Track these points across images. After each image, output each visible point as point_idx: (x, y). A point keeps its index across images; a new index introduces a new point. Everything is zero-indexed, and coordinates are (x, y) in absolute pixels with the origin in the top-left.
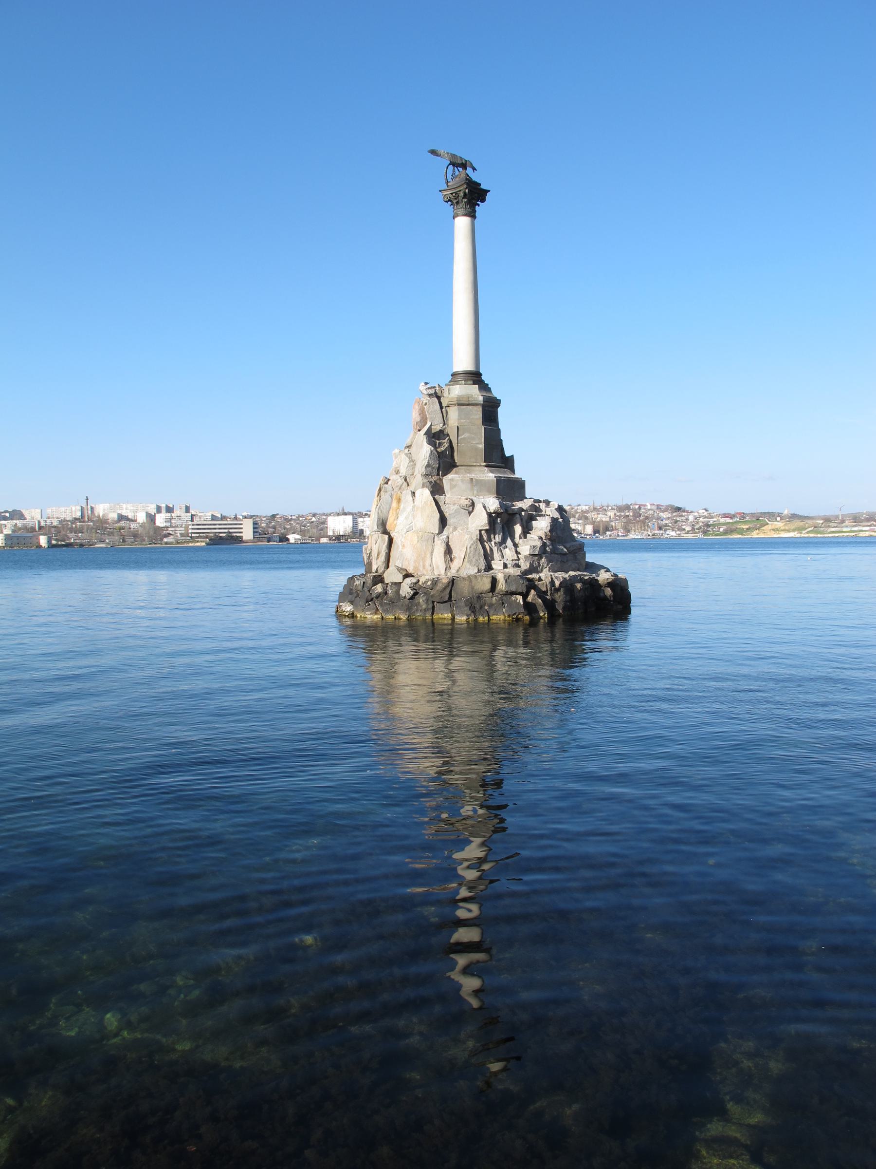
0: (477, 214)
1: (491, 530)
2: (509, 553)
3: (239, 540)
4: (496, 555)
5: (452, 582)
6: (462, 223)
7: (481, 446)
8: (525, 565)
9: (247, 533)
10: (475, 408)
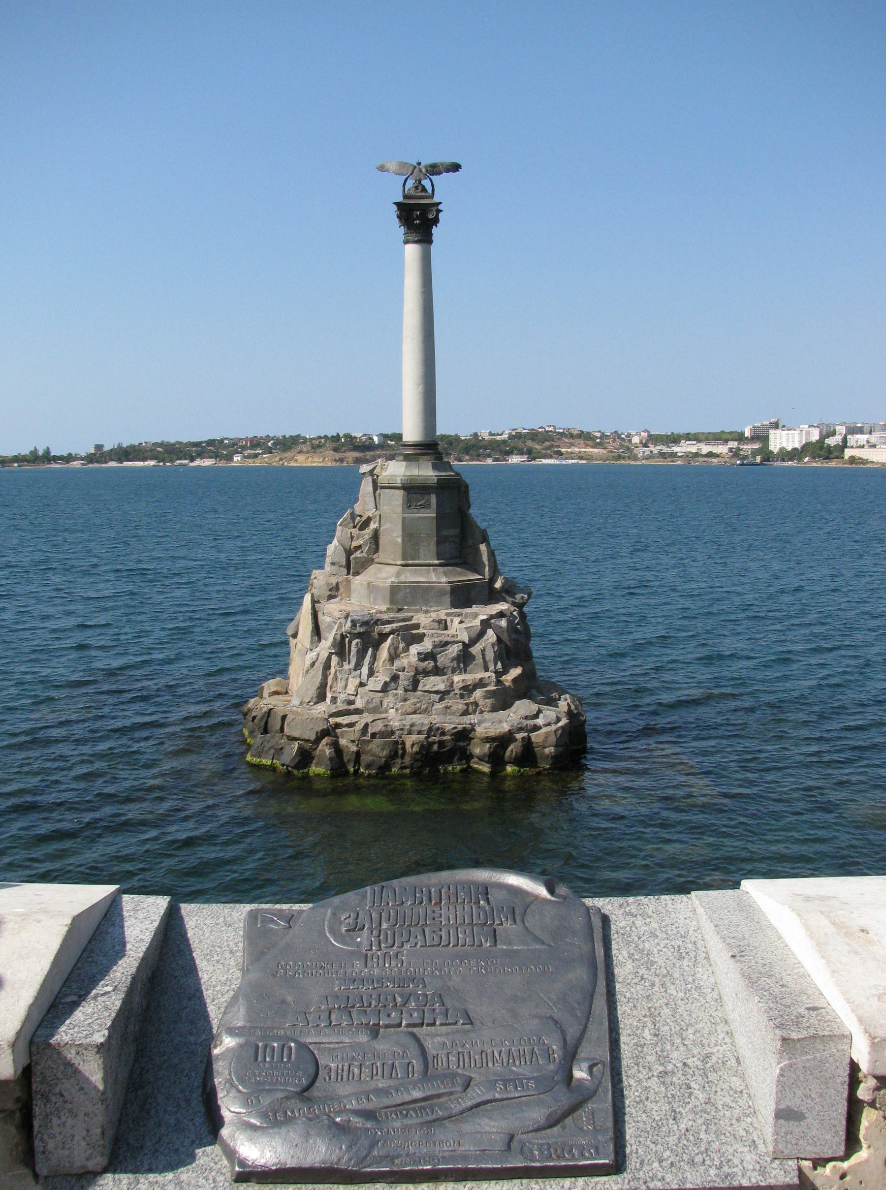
0: (433, 238)
4: (340, 685)
6: (412, 251)
7: (400, 540)
8: (359, 704)
10: (397, 492)
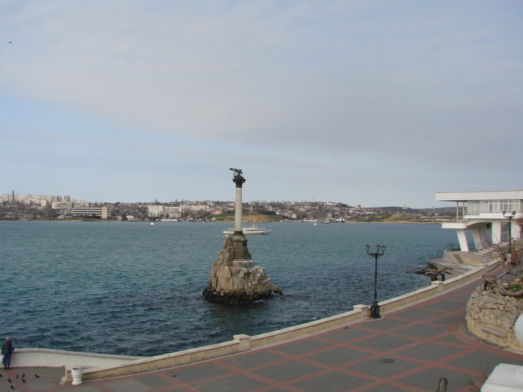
1: (244, 278)
2: (249, 284)
3: (99, 218)
4: (246, 285)
5: (234, 293)
9: (104, 214)
